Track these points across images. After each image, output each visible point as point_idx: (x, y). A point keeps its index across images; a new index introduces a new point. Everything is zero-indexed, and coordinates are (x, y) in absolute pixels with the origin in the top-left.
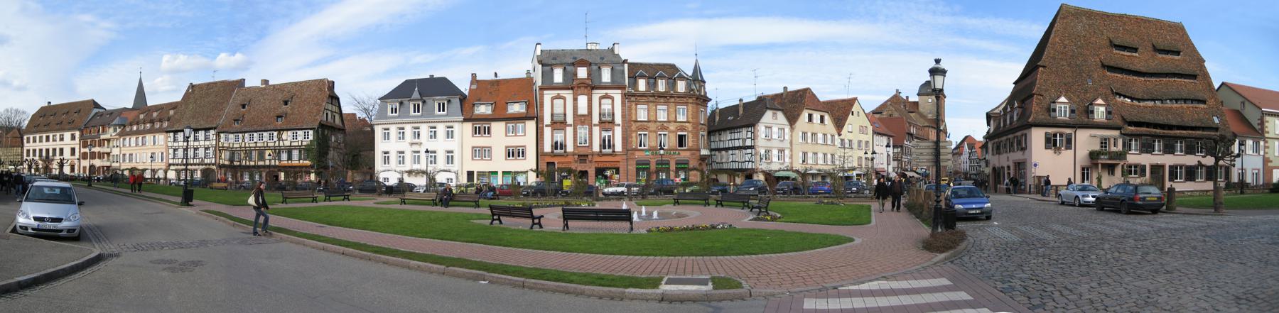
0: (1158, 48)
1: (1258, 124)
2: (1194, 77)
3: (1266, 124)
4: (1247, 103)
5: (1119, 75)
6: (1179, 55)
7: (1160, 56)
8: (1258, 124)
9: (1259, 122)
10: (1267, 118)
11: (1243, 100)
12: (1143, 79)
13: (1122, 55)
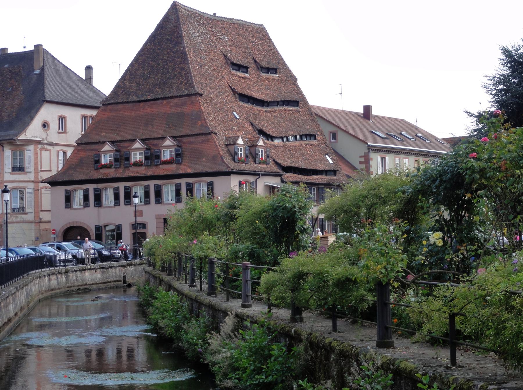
0: (264, 65)
1: (361, 163)
2: (295, 103)
3: (371, 163)
4: (340, 135)
5: (247, 106)
6: (276, 73)
7: (264, 75)
8: (361, 163)
9: (363, 159)
10: (372, 155)
11: (333, 129)
12: (264, 109)
13: (239, 77)
